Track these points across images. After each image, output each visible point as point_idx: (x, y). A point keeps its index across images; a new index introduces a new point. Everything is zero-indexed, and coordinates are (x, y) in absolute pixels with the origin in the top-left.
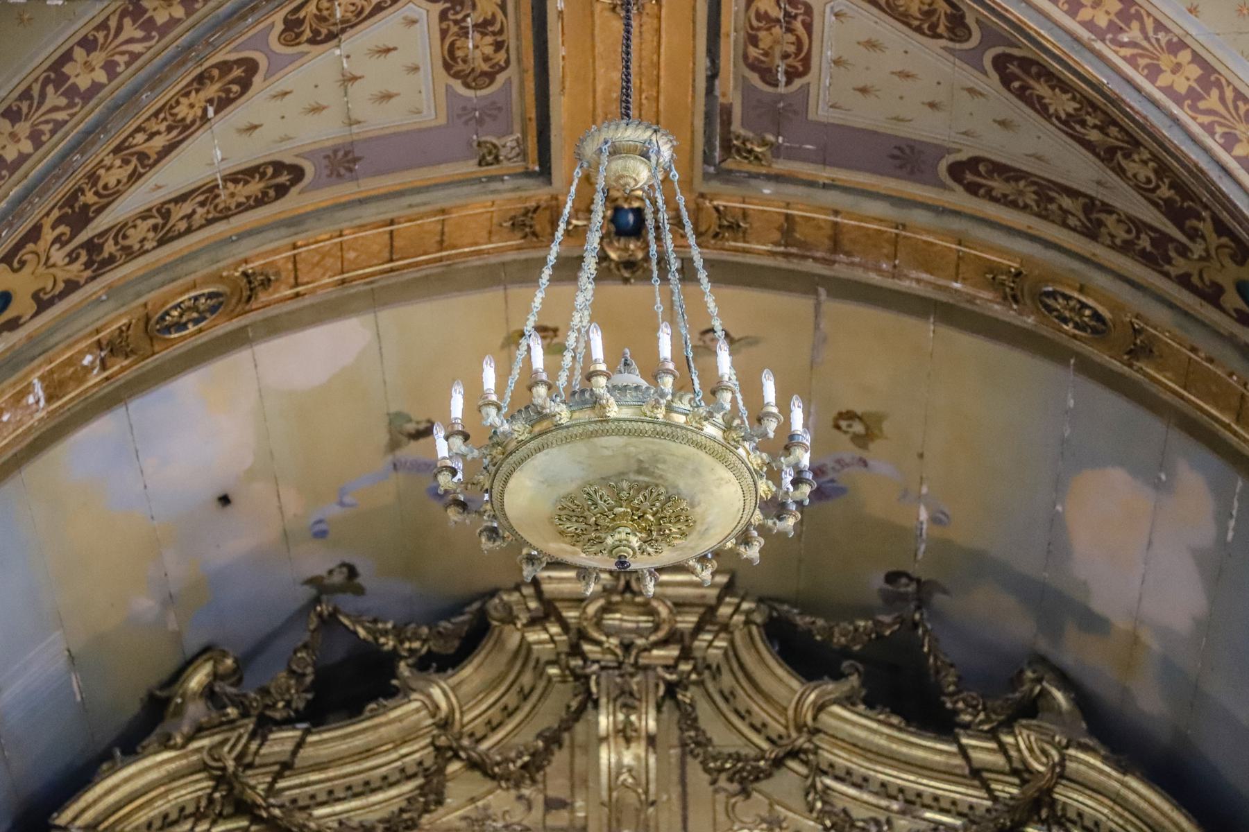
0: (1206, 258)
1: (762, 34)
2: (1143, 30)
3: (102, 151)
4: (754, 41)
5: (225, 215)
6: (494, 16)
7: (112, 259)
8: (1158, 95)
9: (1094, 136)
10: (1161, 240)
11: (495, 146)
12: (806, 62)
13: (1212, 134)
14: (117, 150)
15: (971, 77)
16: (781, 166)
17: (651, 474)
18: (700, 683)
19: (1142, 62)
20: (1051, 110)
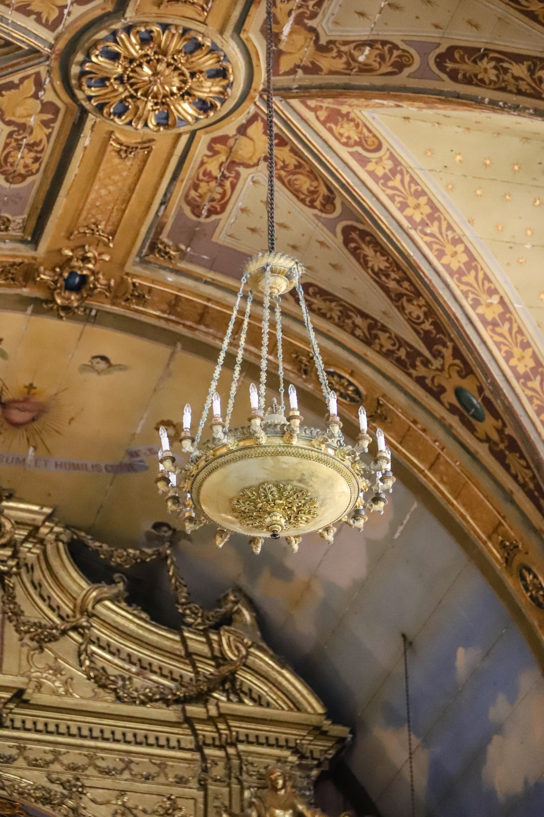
0: (441, 370)
1: (203, 184)
2: (440, 228)
4: (196, 187)
6: (41, 141)
8: (440, 269)
9: (392, 285)
10: (414, 354)
11: (8, 220)
13: (467, 297)
15: (324, 235)
17: (306, 483)
18: (18, 574)
19: (436, 247)
20: (370, 264)
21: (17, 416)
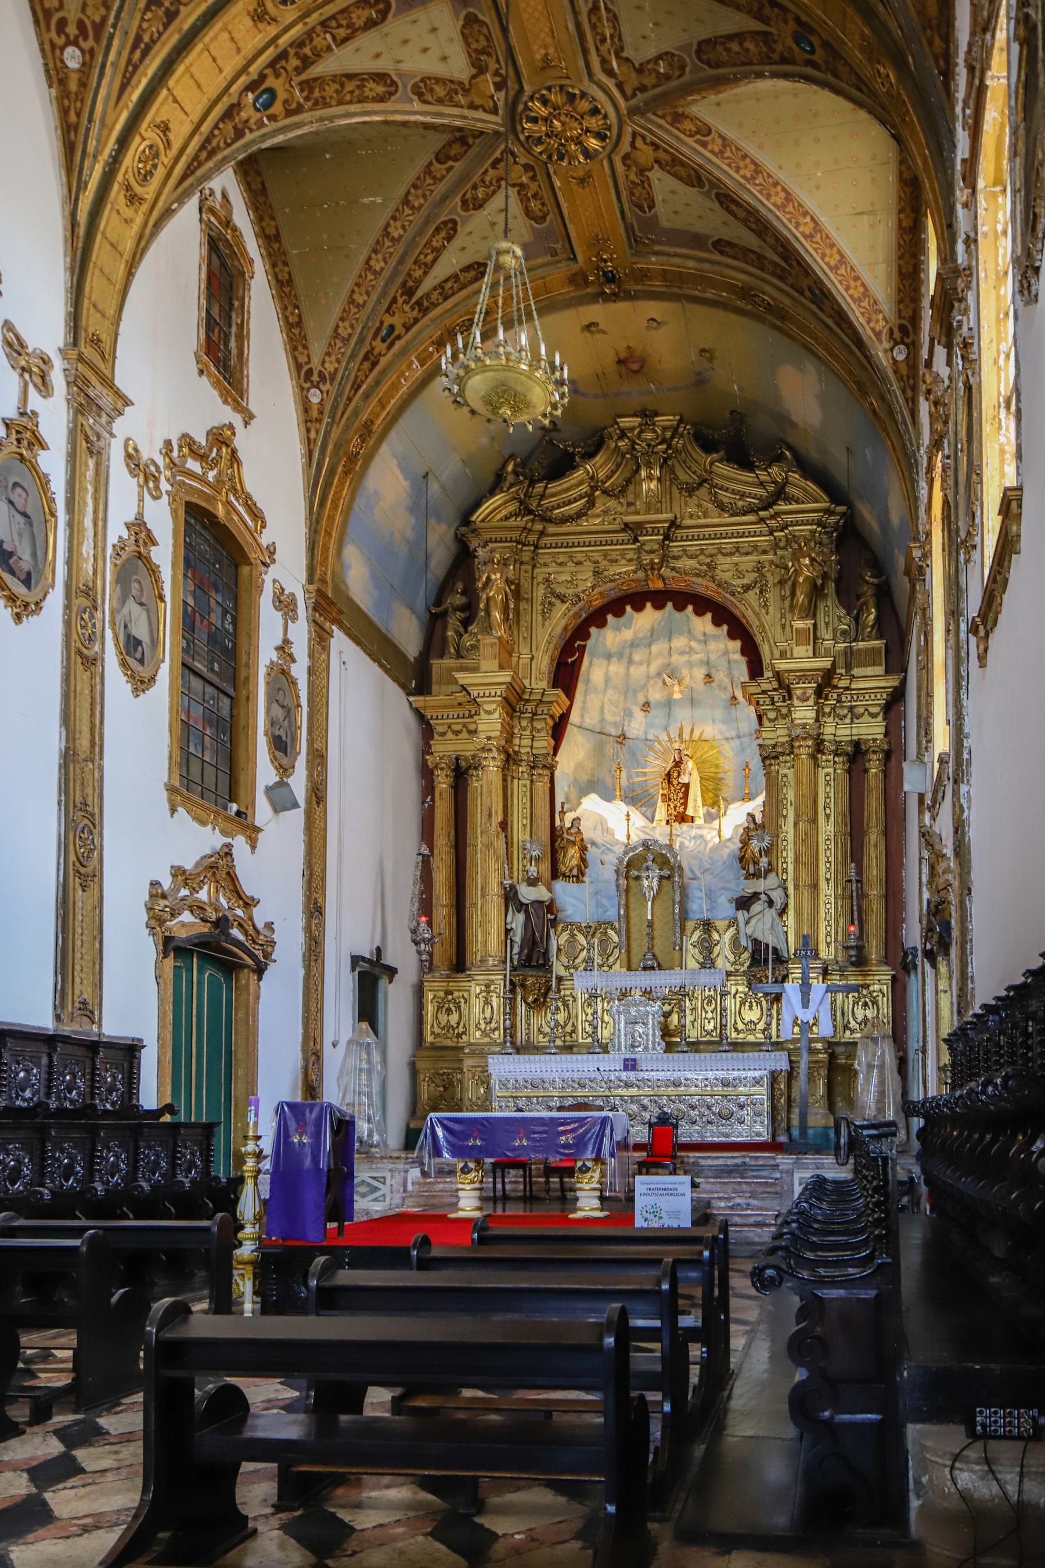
3: (409, 264)
4: (632, 194)
5: (464, 287)
7: (427, 308)
12: (653, 201)
14: (415, 263)
16: (656, 248)
21: (635, 367)
